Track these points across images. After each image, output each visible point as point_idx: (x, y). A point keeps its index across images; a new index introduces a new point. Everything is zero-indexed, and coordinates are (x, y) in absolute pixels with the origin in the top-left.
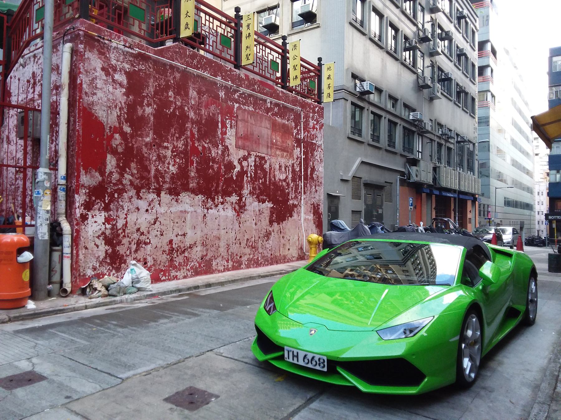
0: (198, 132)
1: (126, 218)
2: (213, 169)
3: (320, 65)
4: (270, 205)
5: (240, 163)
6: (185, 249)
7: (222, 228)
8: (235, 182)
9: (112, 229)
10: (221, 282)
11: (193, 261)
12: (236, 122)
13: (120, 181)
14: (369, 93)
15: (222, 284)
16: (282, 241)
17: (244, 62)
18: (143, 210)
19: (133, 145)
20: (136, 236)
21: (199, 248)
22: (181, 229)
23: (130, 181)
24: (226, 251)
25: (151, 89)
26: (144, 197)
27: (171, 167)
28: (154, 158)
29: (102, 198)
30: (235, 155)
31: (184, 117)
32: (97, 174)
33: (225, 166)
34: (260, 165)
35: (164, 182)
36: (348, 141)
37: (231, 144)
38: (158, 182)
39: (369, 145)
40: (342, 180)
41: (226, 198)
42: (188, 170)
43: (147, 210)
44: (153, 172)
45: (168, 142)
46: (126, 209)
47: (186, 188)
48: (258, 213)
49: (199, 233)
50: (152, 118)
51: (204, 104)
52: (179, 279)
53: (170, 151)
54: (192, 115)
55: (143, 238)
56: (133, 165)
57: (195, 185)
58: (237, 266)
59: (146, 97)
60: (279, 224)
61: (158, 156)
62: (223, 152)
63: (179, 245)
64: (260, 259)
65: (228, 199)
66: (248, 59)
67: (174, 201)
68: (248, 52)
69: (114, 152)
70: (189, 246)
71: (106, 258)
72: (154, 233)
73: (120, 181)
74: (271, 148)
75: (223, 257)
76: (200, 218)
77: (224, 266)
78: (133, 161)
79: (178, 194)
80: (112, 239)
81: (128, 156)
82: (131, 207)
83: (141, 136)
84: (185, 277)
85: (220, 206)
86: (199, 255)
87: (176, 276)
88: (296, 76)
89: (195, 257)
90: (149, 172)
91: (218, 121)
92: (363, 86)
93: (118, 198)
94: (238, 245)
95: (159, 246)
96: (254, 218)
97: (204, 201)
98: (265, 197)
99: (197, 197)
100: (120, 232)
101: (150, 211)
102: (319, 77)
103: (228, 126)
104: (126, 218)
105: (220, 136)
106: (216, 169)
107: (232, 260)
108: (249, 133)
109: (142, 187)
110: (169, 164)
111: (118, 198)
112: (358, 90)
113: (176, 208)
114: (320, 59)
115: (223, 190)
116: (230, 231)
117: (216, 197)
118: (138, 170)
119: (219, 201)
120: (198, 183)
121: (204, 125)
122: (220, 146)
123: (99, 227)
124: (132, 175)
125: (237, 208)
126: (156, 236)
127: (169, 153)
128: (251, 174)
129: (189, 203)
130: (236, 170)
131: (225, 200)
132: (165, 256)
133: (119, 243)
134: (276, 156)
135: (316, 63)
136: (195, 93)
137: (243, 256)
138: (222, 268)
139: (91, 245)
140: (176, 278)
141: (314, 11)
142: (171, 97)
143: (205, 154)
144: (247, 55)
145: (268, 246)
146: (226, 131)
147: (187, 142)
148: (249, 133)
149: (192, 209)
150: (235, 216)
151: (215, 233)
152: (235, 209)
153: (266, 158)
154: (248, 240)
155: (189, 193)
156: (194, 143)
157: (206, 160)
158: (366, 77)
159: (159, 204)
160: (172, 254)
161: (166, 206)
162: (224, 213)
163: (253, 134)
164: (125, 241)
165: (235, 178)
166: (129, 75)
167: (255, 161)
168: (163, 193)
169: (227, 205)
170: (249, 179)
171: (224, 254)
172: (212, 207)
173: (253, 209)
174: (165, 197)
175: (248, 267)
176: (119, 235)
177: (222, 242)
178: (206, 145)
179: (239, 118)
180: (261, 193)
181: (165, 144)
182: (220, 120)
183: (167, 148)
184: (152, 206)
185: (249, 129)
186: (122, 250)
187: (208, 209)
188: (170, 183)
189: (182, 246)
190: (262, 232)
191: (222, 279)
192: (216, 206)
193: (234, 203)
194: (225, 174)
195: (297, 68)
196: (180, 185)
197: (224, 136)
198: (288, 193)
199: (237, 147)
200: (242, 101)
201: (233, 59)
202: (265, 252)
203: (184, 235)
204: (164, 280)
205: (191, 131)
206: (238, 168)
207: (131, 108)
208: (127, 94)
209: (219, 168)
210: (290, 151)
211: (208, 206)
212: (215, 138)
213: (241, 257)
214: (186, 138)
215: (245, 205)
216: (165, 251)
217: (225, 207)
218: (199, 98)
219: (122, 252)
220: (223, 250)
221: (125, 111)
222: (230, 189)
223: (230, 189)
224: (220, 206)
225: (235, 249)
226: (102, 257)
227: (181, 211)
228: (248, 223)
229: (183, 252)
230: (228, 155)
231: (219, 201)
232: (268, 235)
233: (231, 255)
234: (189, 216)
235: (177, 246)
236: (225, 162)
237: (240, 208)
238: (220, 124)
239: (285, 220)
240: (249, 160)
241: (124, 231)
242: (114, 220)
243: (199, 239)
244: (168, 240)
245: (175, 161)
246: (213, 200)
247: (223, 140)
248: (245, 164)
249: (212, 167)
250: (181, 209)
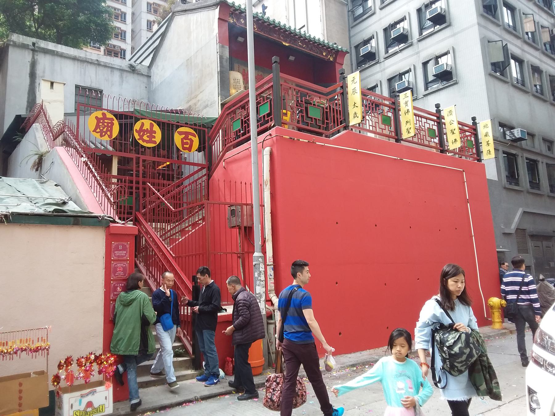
3: (475, 124)
14: (520, 139)
17: (405, 136)
36: (504, 191)
39: (528, 192)
40: (505, 234)
66: (409, 133)
68: (408, 126)
88: (455, 140)
92: (513, 134)
102: (476, 135)
112: (508, 138)
114: (474, 119)
135: (470, 123)
141: (449, 69)
144: (407, 129)
158: (514, 123)
195: (455, 132)
201: (393, 134)
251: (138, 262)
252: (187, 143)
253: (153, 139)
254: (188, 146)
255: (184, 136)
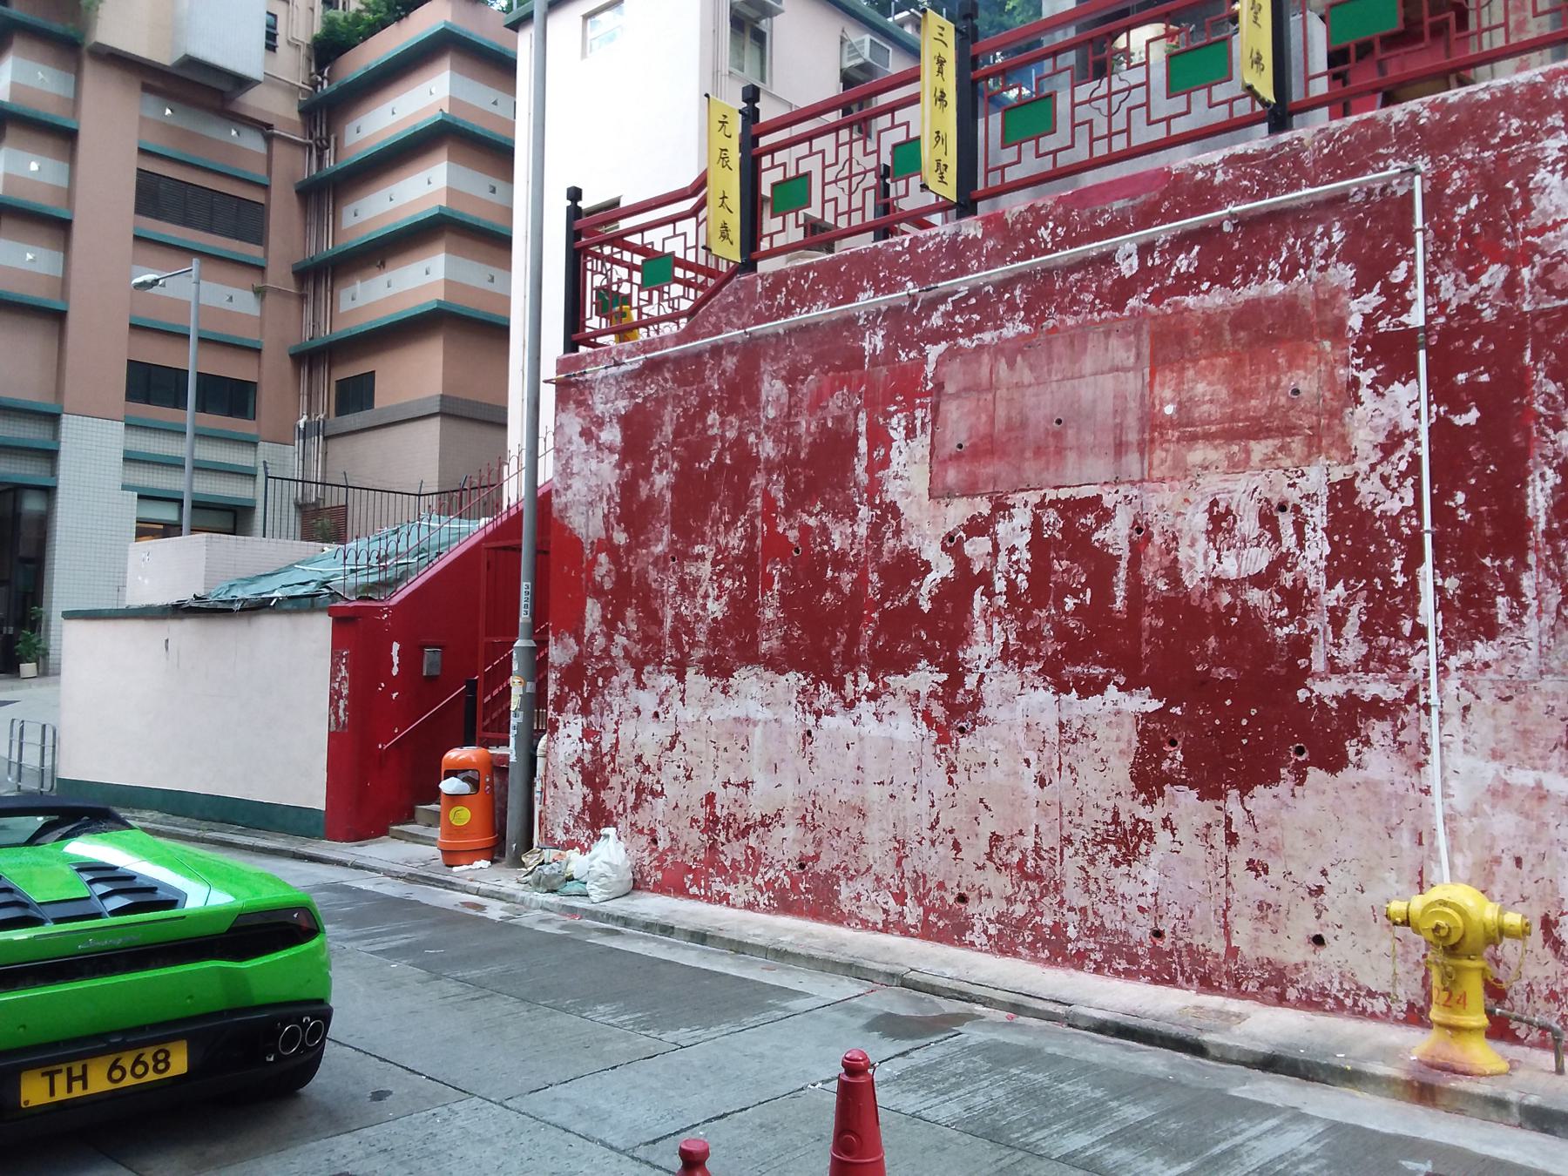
0: (786, 490)
1: (616, 731)
2: (837, 590)
4: (1143, 702)
5: (952, 545)
6: (748, 827)
7: (871, 775)
8: (927, 620)
9: (593, 752)
10: (740, 943)
11: (771, 866)
12: (935, 409)
13: (606, 651)
15: (739, 947)
16: (1247, 884)
18: (647, 714)
19: (630, 568)
20: (634, 772)
21: (791, 831)
22: (737, 768)
23: (625, 648)
24: (890, 862)
25: (668, 429)
26: (649, 683)
27: (712, 606)
28: (673, 589)
29: (576, 687)
30: (927, 528)
31: (746, 461)
32: (572, 641)
33: (884, 571)
34: (1070, 534)
35: (693, 645)
37: (907, 494)
38: (679, 648)
41: (890, 679)
42: (757, 605)
43: (656, 715)
44: (668, 624)
45: (704, 542)
46: (616, 713)
47: (749, 655)
48: (1053, 735)
49: (790, 790)
50: (668, 496)
51: (805, 404)
52: (734, 906)
53: (708, 563)
54: (768, 449)
55: (648, 779)
56: (630, 613)
57: (775, 643)
58: (948, 926)
59: (657, 452)
60: (1210, 791)
61: (682, 581)
62: (875, 530)
63: (733, 810)
64: (1072, 932)
65: (896, 681)
67: (717, 693)
69: (598, 592)
70: (759, 818)
71: (583, 811)
72: (671, 770)
73: (606, 651)
74: (1144, 447)
75: (878, 880)
76: (793, 742)
77: (886, 911)
78: (630, 605)
79: (727, 673)
80: (594, 774)
81: (629, 593)
82: (625, 706)
83: (646, 545)
84: (750, 906)
85: (865, 708)
86: (793, 852)
87: (727, 896)
89: (779, 856)
90: (661, 623)
91: (857, 434)
93: (604, 687)
94: (945, 851)
95: (682, 805)
96: (1033, 756)
97: (804, 690)
98: (1098, 671)
99: (783, 678)
100: (607, 759)
101: (662, 716)
103: (898, 435)
104: (616, 731)
105: (863, 478)
106: (847, 589)
107: (920, 900)
108: (1000, 425)
109: (646, 662)
110: (706, 596)
111: (604, 687)
113: (725, 710)
115: (872, 651)
116: (908, 793)
117: (849, 677)
118: (639, 622)
119: (861, 689)
120: (785, 639)
121: (806, 464)
122: (864, 512)
123: (574, 747)
124: (628, 636)
125: (938, 711)
126: (676, 778)
127: (706, 569)
128: (1012, 584)
129: (762, 698)
130: (930, 577)
131: (886, 686)
132: (696, 833)
133: (605, 784)
134: (1181, 470)
136: (779, 384)
137: (972, 896)
138: (878, 917)
139: (562, 782)
140: (724, 899)
142: (712, 426)
143: (807, 549)
145: (1124, 887)
146: (887, 454)
147: (754, 527)
148: (1000, 425)
149: (767, 714)
150: (928, 744)
151: (846, 792)
152: (927, 717)
153: (1108, 502)
154: (995, 839)
155: (759, 670)
156: (772, 525)
157: (811, 566)
159: (682, 700)
160: (713, 831)
161: (699, 706)
162: (882, 730)
163: (1024, 425)
164: (615, 781)
165: (926, 606)
166: (625, 421)
167: (1036, 526)
168: (690, 673)
169: (890, 704)
170: (1001, 601)
171: (887, 870)
172: (835, 707)
173: (1021, 720)
174: (697, 682)
175: (1003, 945)
176: (604, 767)
177: (875, 826)
178: (812, 522)
179: (950, 388)
180: (1076, 650)
181: (698, 549)
182: (862, 428)
183: (701, 557)
184: (666, 704)
185: (1001, 412)
186: (610, 799)
187: (818, 714)
188: (707, 646)
189: (740, 815)
190: (1085, 820)
191: (787, 941)
192: (850, 705)
193: (924, 692)
194: (884, 600)
196: (734, 648)
197: (880, 473)
198: (1301, 646)
199: (939, 493)
200: (967, 323)
202: (1102, 909)
203: (745, 785)
204: (695, 897)
205: (766, 493)
206: (943, 568)
207: (628, 488)
208: (620, 465)
209: (862, 581)
210: (1306, 421)
211: (817, 705)
212: (844, 488)
213: (962, 899)
214: (751, 520)
215: (978, 703)
216: (696, 821)
217: (886, 709)
218: (792, 392)
219: (609, 805)
220: (877, 853)
221: (617, 499)
222: (905, 648)
223: (905, 648)
224: (865, 708)
225: (932, 861)
226: (577, 809)
227: (736, 719)
228: (996, 774)
229: (744, 833)
230: (898, 533)
231: (861, 689)
232: (1128, 841)
233: (915, 882)
234: (757, 734)
235: (725, 812)
236: (886, 557)
237: (955, 713)
238: (863, 444)
239: (1272, 779)
240: (1002, 528)
241: (613, 759)
242: (597, 733)
243: (790, 804)
244: (703, 794)
245: (720, 587)
246: (838, 686)
247: (875, 487)
248: (977, 548)
249: (834, 585)
250: (735, 713)
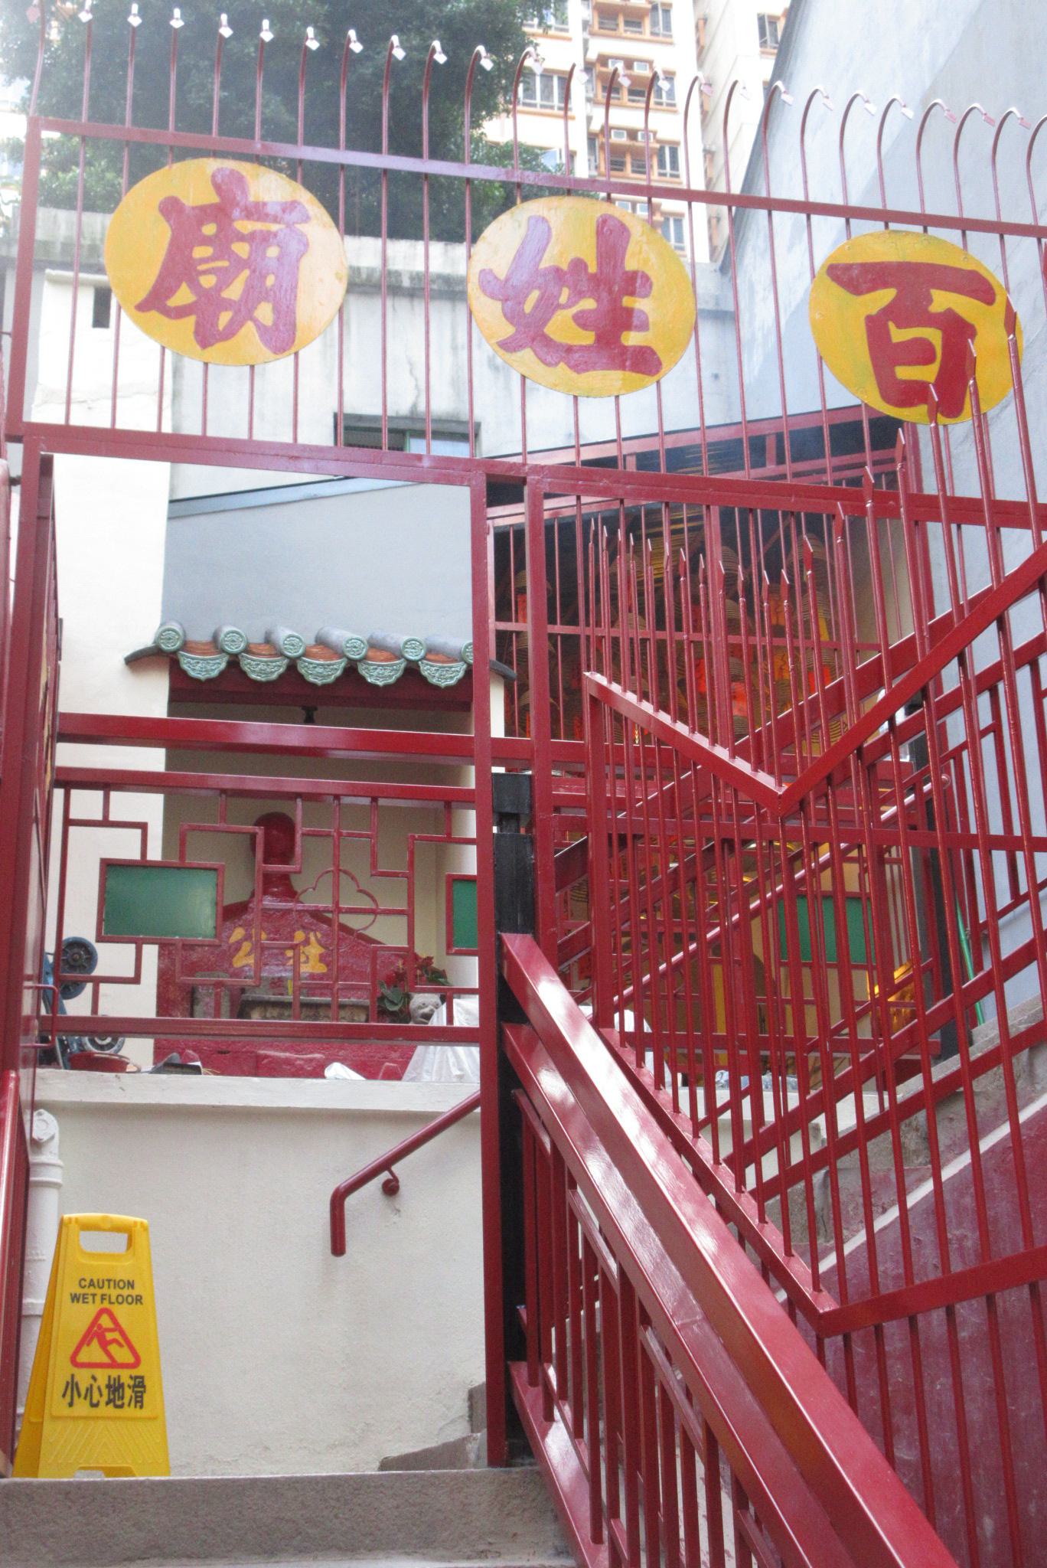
251: (529, 1399)
252: (921, 353)
253: (632, 339)
254: (928, 373)
255: (885, 297)
